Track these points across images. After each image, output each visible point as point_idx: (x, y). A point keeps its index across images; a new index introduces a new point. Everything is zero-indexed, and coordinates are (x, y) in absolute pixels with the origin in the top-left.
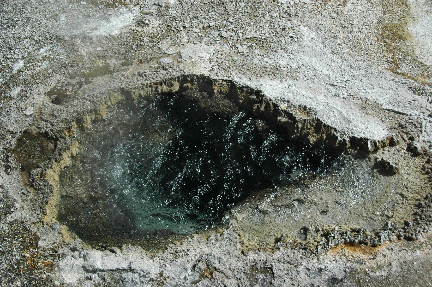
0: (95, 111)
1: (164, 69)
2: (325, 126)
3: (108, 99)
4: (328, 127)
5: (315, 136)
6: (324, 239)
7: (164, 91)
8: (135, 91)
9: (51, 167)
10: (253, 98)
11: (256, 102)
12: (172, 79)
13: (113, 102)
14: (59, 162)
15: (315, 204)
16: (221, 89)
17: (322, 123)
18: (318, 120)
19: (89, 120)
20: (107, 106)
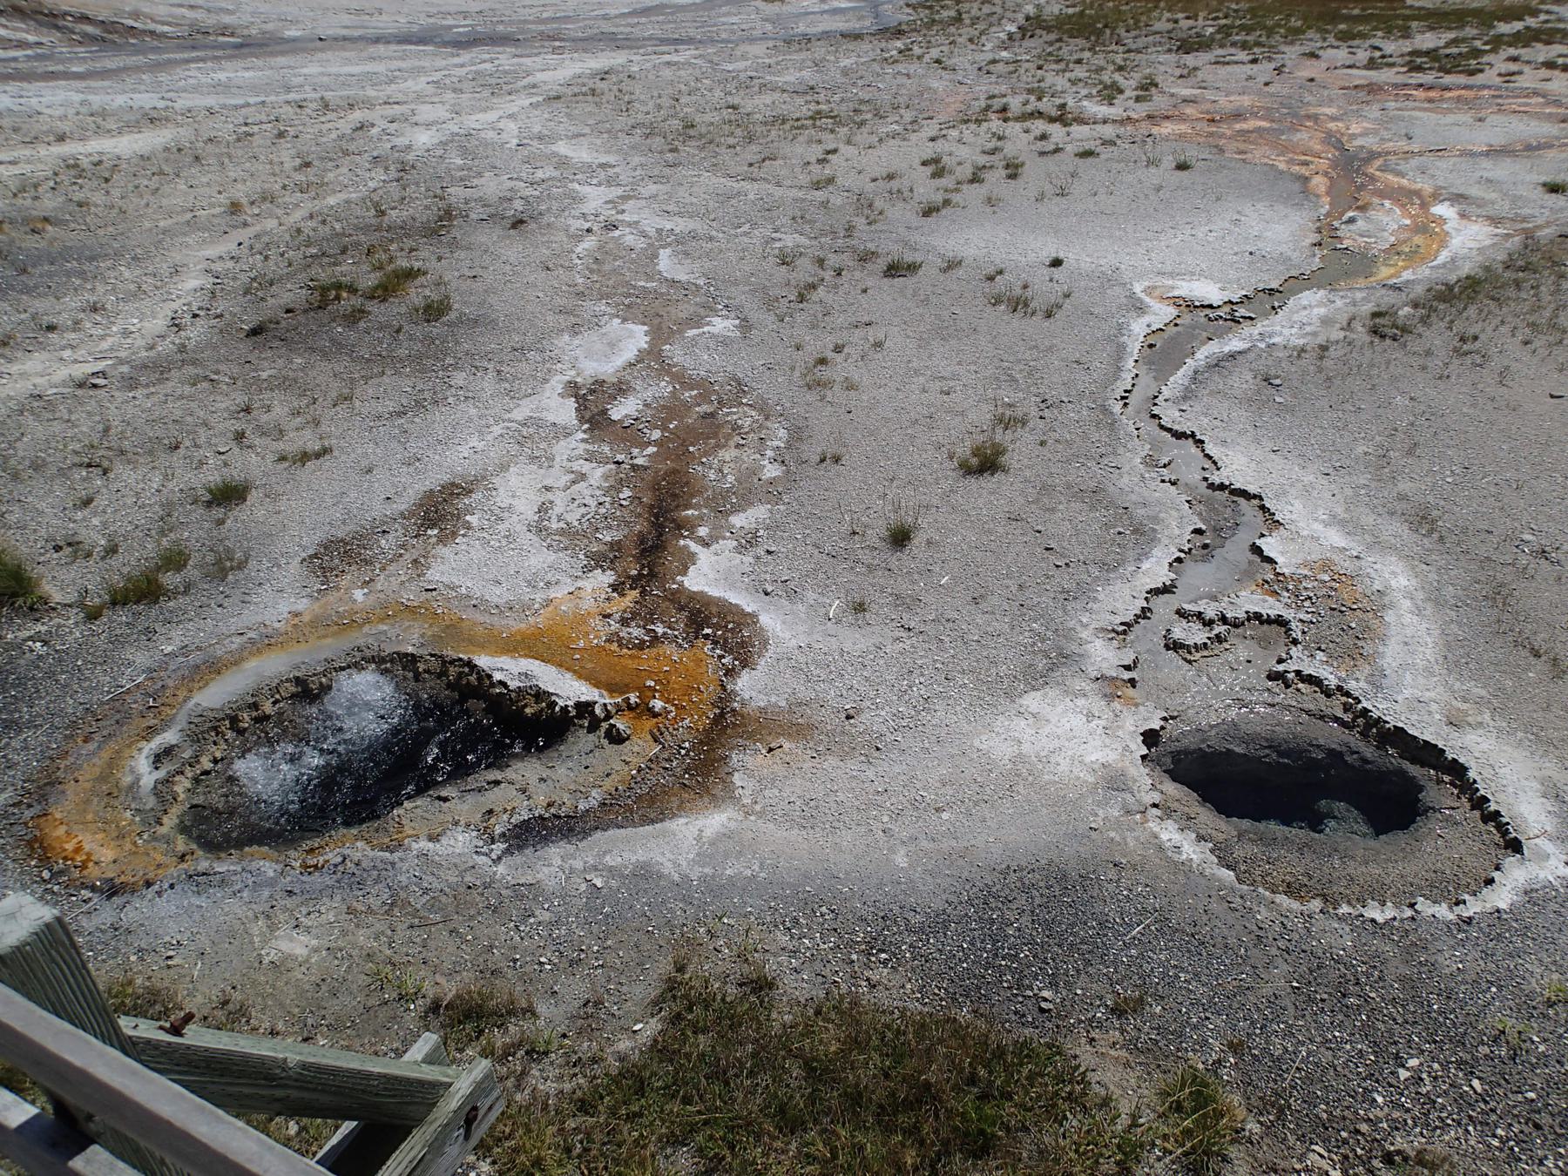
0: (255, 706)
19: (247, 718)
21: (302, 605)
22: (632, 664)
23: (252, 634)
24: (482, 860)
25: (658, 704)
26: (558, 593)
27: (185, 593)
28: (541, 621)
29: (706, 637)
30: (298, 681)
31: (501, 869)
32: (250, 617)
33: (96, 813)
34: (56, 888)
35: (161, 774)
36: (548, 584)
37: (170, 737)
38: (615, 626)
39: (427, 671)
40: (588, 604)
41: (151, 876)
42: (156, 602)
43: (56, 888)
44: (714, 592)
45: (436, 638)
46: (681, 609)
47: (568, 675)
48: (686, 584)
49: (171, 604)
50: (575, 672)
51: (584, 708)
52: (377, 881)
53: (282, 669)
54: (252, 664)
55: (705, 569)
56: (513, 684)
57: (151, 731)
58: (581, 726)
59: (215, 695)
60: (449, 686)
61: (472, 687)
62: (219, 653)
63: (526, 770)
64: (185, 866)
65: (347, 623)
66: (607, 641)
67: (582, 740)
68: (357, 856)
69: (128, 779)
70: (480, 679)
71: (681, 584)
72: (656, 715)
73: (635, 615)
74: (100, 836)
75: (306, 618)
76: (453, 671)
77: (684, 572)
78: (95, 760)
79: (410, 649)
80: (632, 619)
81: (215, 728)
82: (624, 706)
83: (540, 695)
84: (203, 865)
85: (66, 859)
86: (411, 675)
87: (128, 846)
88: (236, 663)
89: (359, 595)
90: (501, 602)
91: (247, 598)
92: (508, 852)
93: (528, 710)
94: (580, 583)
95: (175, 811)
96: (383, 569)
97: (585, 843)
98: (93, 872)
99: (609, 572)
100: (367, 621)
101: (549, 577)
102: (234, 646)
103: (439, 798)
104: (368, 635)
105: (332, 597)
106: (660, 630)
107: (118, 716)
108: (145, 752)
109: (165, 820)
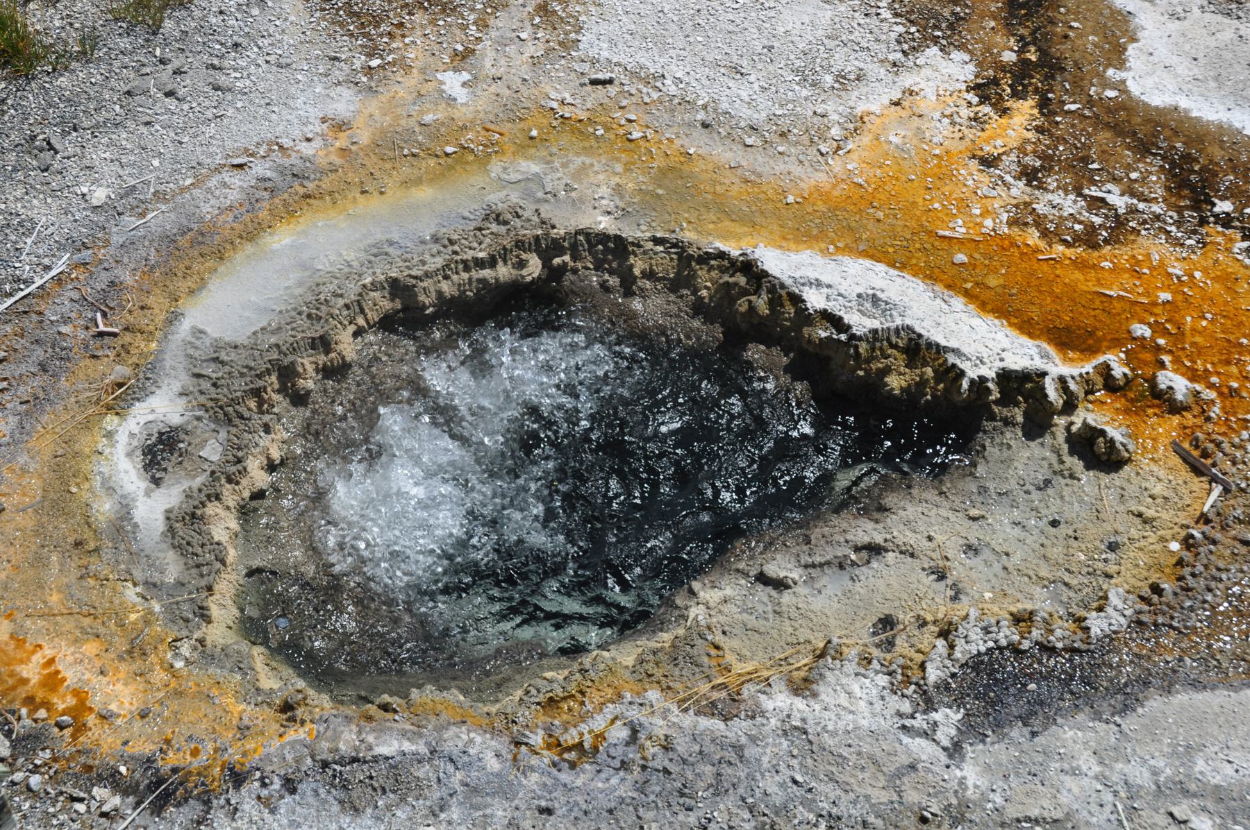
0: (323, 343)
1: (498, 219)
2: (930, 345)
3: (357, 310)
4: (939, 350)
5: (904, 374)
6: (941, 643)
8: (425, 284)
11: (744, 293)
12: (520, 245)
13: (369, 316)
14: (237, 483)
15: (912, 555)
16: (651, 265)
17: (920, 336)
18: (909, 329)
19: (310, 368)
21: (344, 103)
22: (1085, 283)
23: (260, 168)
24: (921, 748)
25: (1177, 383)
26: (873, 100)
27: (84, 56)
28: (854, 164)
29: (1226, 221)
30: (396, 288)
31: (970, 775)
32: (239, 129)
33: (65, 589)
34: (35, 780)
35: (170, 497)
36: (841, 77)
37: (163, 406)
38: (1019, 189)
39: (650, 275)
40: (940, 133)
41: (234, 755)
42: (29, 78)
43: (35, 780)
44: (1207, 110)
45: (650, 201)
46: (1144, 148)
47: (958, 303)
48: (1134, 88)
49: (63, 81)
50: (967, 294)
51: (1020, 385)
52: (718, 790)
53: (351, 256)
54: (281, 239)
55: (1163, 53)
56: (861, 323)
57: (121, 397)
58: (1007, 422)
59: (233, 306)
60: (698, 308)
61: (749, 317)
62: (207, 210)
63: (923, 519)
64: (297, 734)
65: (447, 151)
66: (1012, 223)
67: (1018, 458)
68: (659, 727)
69: (104, 508)
70: (775, 302)
71: (1121, 86)
72: (1176, 408)
73: (1048, 163)
74: (91, 648)
75: (364, 137)
76: (706, 281)
77: (1117, 56)
78: (22, 459)
79: (604, 224)
80: (1048, 170)
81: (257, 393)
82: (1099, 381)
83: (916, 349)
84: (348, 740)
85: (29, 701)
86: (613, 281)
87: (159, 676)
88: (250, 235)
89: (453, 82)
90: (760, 117)
91: (223, 80)
92: (970, 730)
93: (895, 383)
94: (907, 80)
95: (227, 584)
96: (483, 25)
97: (1129, 723)
98: (104, 741)
99: (958, 56)
100: (492, 149)
101: (840, 60)
102: (233, 196)
103: (763, 579)
104: (503, 183)
105: (403, 87)
106: (1119, 201)
107: (39, 354)
108: (122, 438)
109: (215, 611)
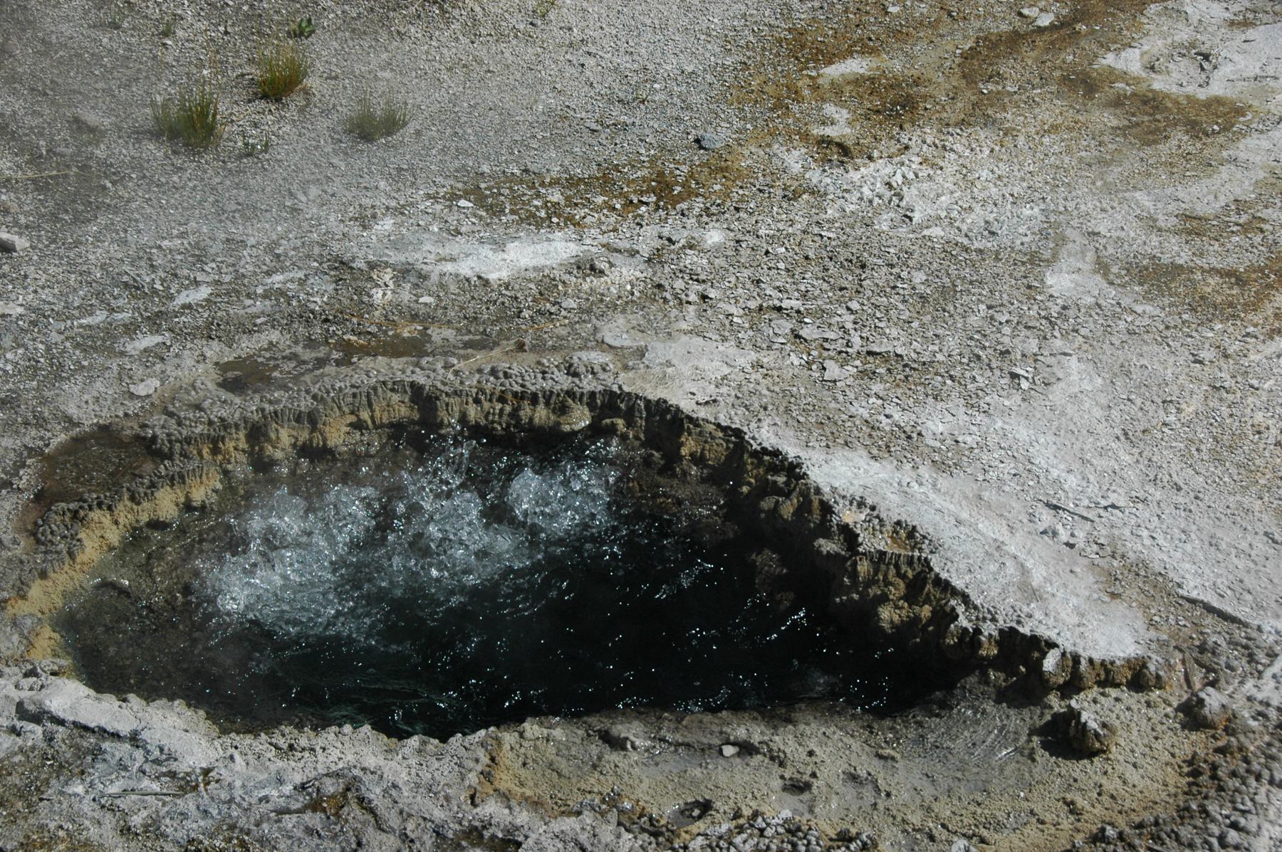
2: (938, 581)
5: (901, 608)
7: (536, 420)
9: (110, 508)
10: (775, 482)
14: (138, 504)
20: (352, 419)
